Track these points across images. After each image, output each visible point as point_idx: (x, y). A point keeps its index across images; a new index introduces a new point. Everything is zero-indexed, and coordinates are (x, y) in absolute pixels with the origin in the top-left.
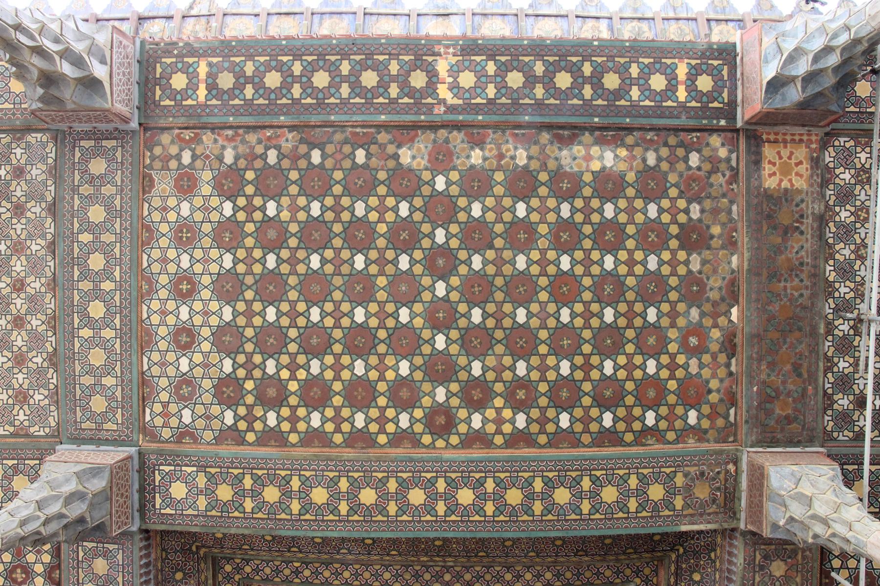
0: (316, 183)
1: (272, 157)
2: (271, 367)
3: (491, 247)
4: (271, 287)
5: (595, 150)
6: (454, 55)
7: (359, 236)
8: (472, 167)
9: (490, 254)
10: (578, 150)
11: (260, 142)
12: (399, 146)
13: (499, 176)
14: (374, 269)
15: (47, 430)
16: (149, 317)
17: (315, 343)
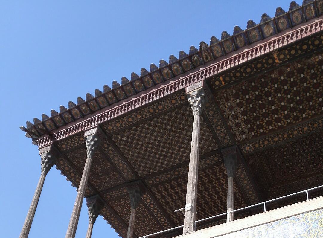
0: (255, 89)
1: (244, 88)
2: (258, 123)
3: (298, 85)
4: (253, 110)
5: (316, 57)
6: (277, 52)
7: (268, 94)
8: (289, 72)
9: (298, 86)
10: (312, 58)
11: (240, 86)
12: (271, 75)
13: (295, 71)
14: (273, 99)
15: (217, 148)
16: (230, 124)
17: (265, 115)
